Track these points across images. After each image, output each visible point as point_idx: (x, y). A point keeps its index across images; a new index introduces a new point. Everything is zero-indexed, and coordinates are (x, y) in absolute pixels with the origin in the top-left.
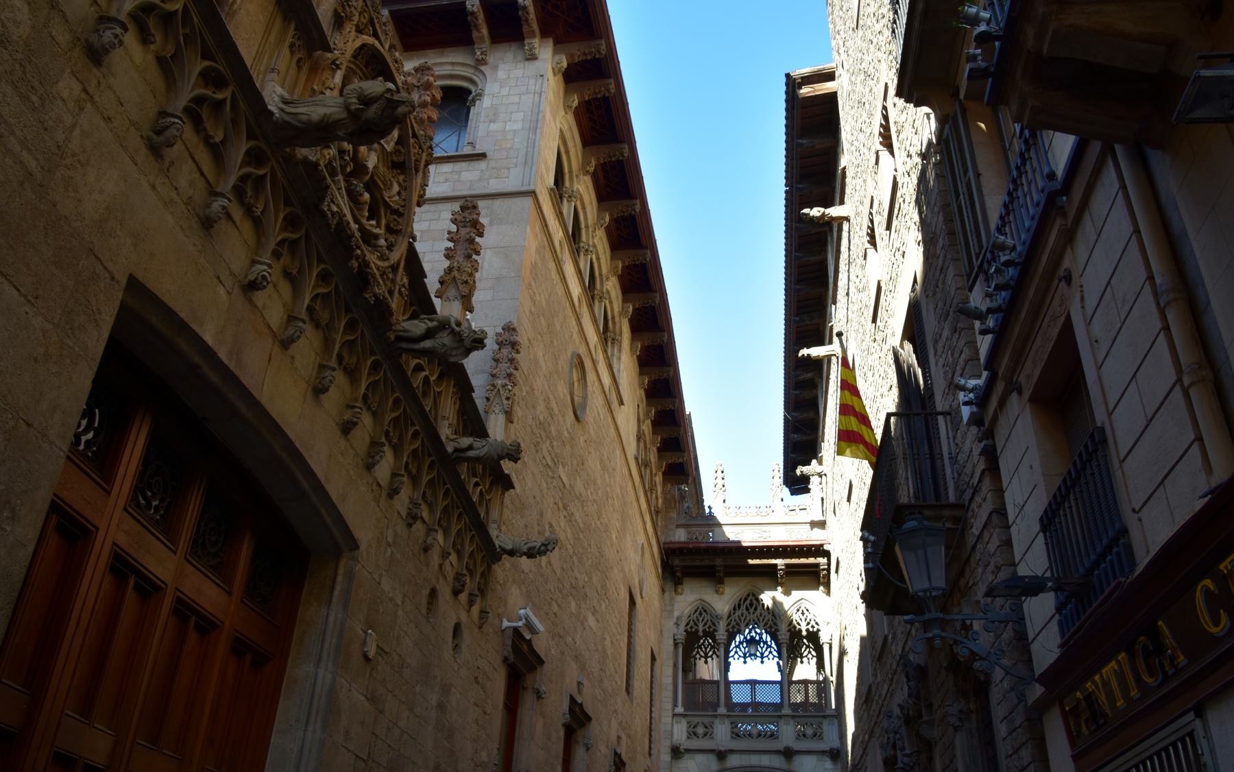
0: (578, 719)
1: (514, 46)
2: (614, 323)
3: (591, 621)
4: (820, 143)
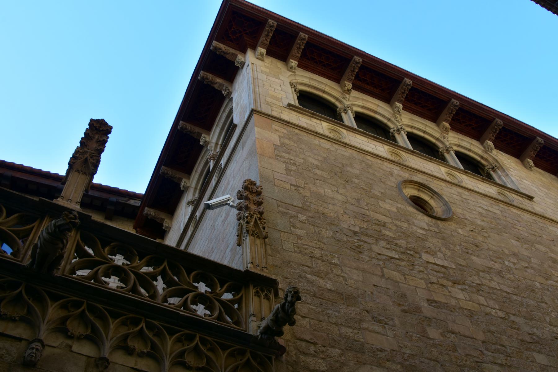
2: (486, 160)
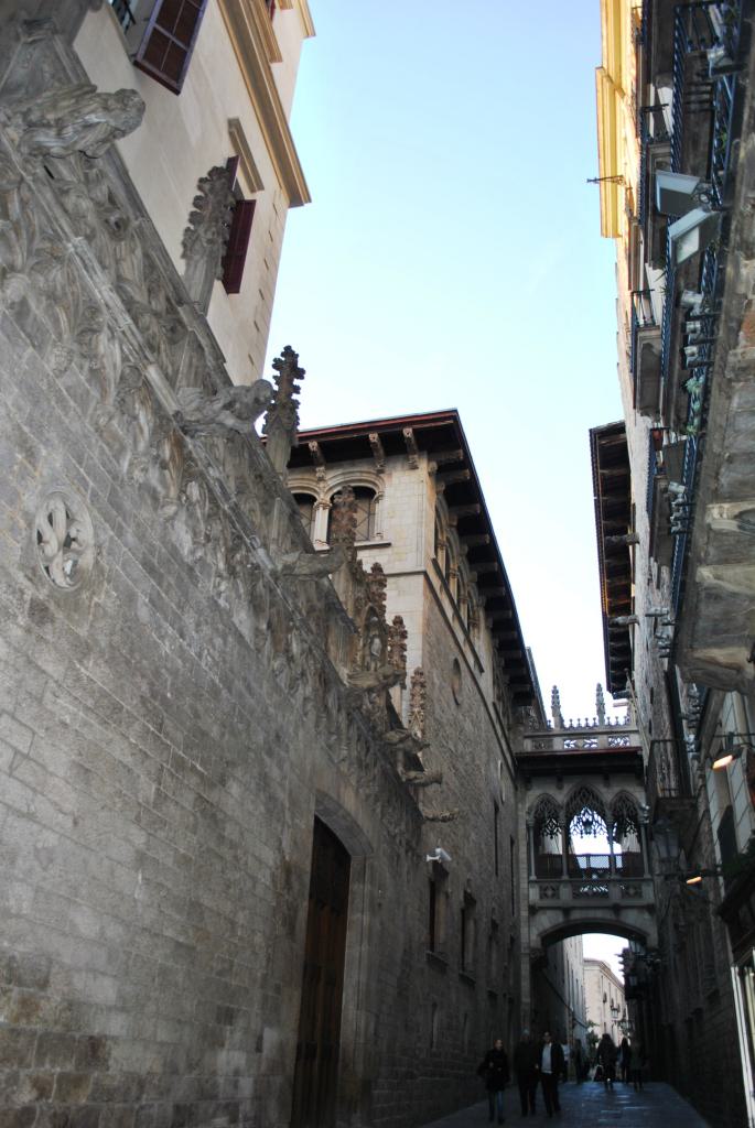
1: (401, 457)
4: (620, 471)
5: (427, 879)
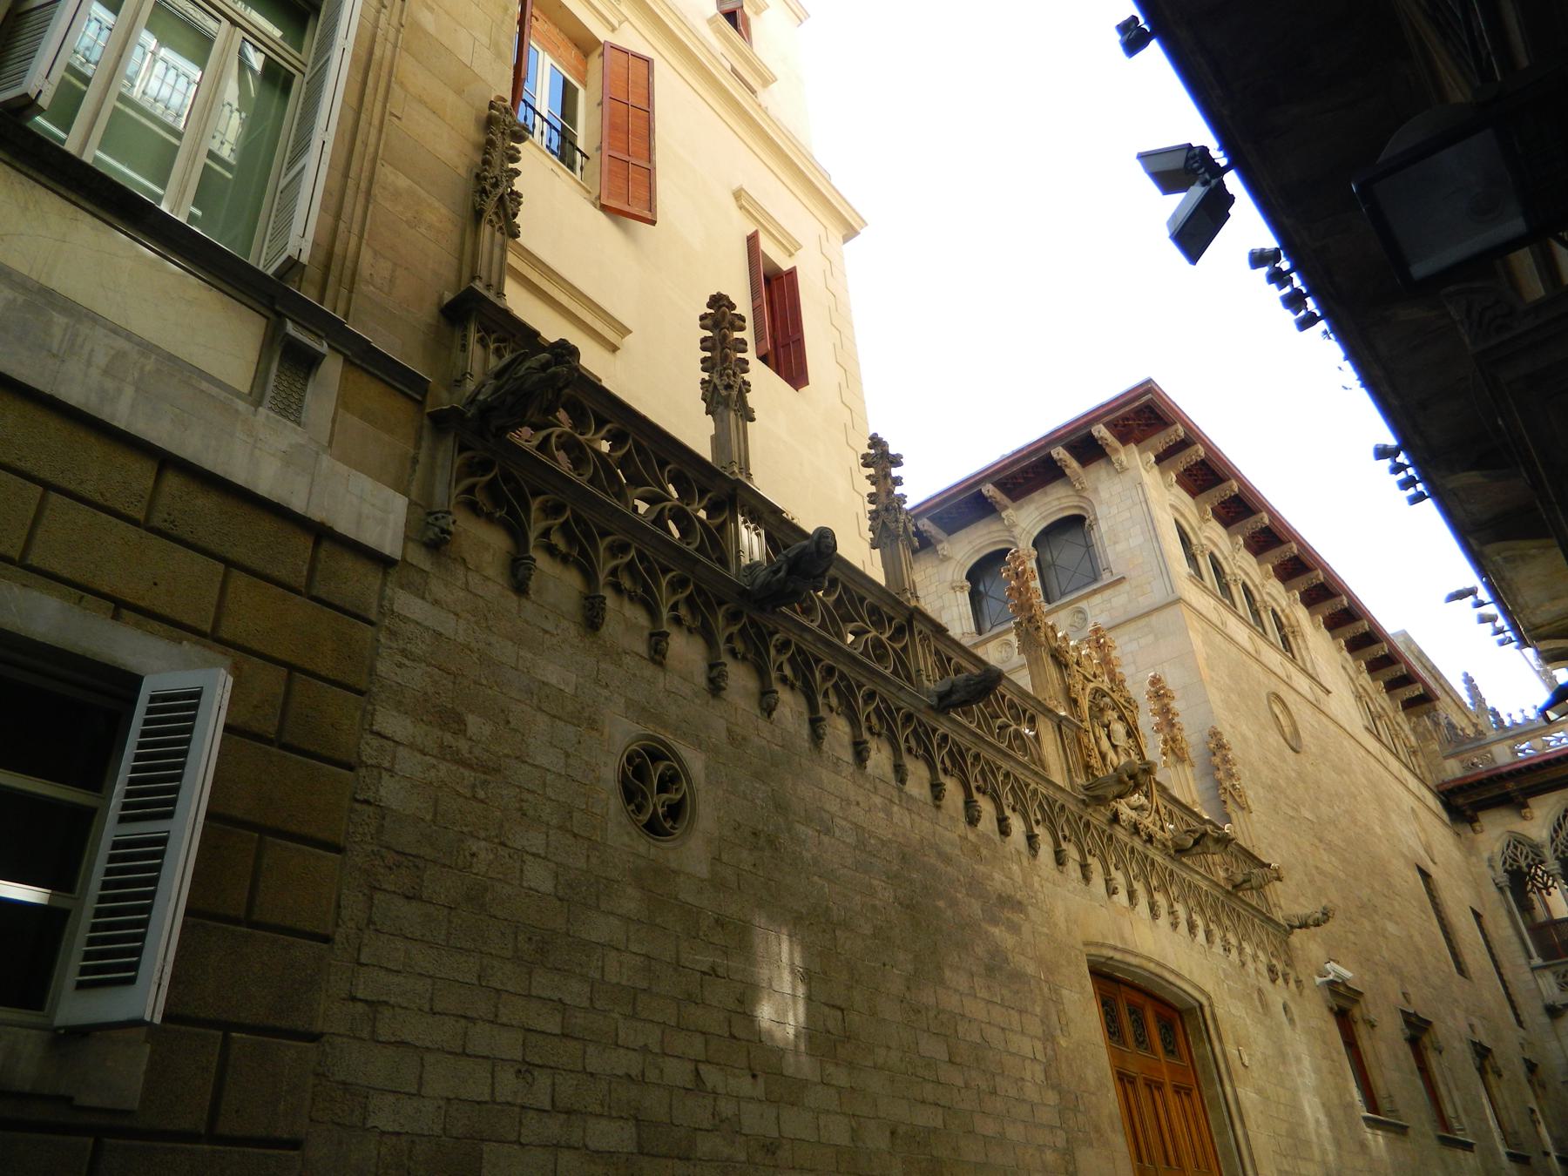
0: (1417, 1029)
2: (1287, 617)
3: (1391, 928)
5: (1326, 1012)
